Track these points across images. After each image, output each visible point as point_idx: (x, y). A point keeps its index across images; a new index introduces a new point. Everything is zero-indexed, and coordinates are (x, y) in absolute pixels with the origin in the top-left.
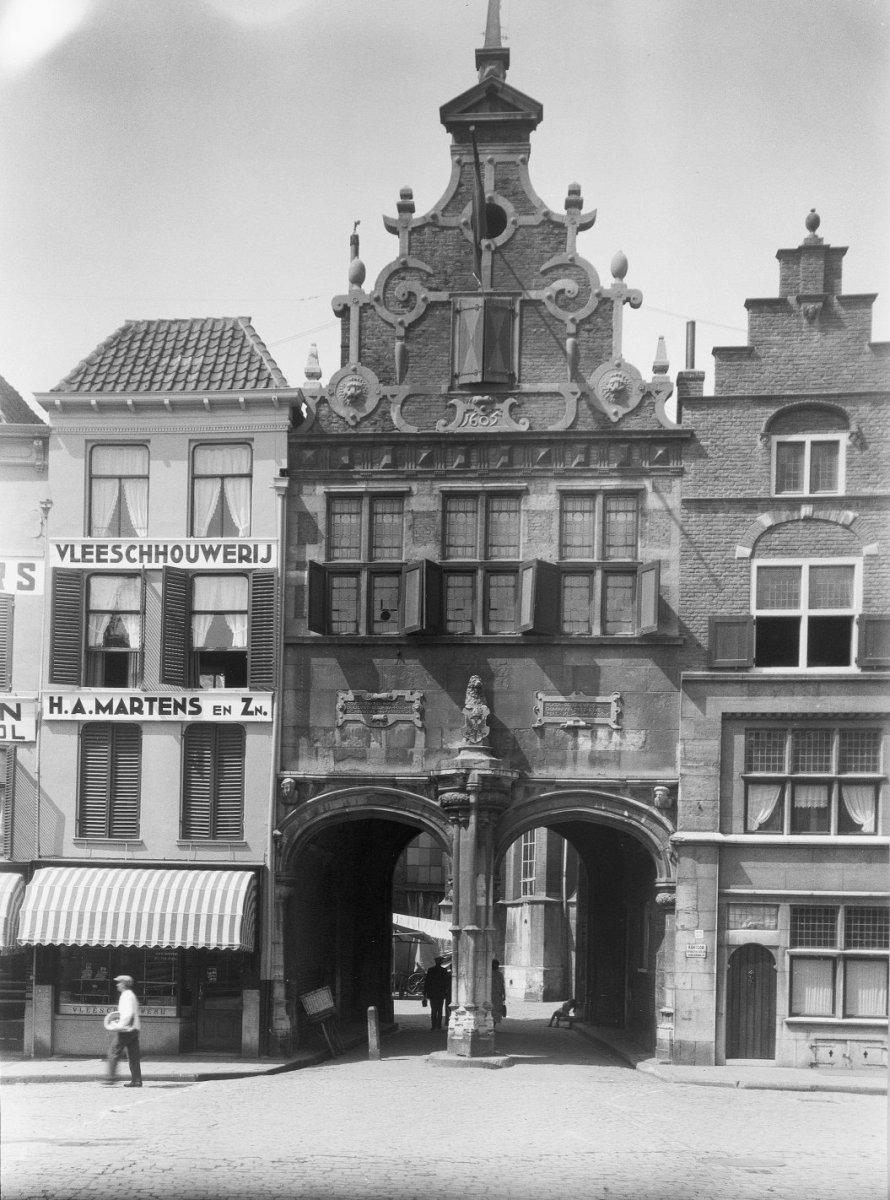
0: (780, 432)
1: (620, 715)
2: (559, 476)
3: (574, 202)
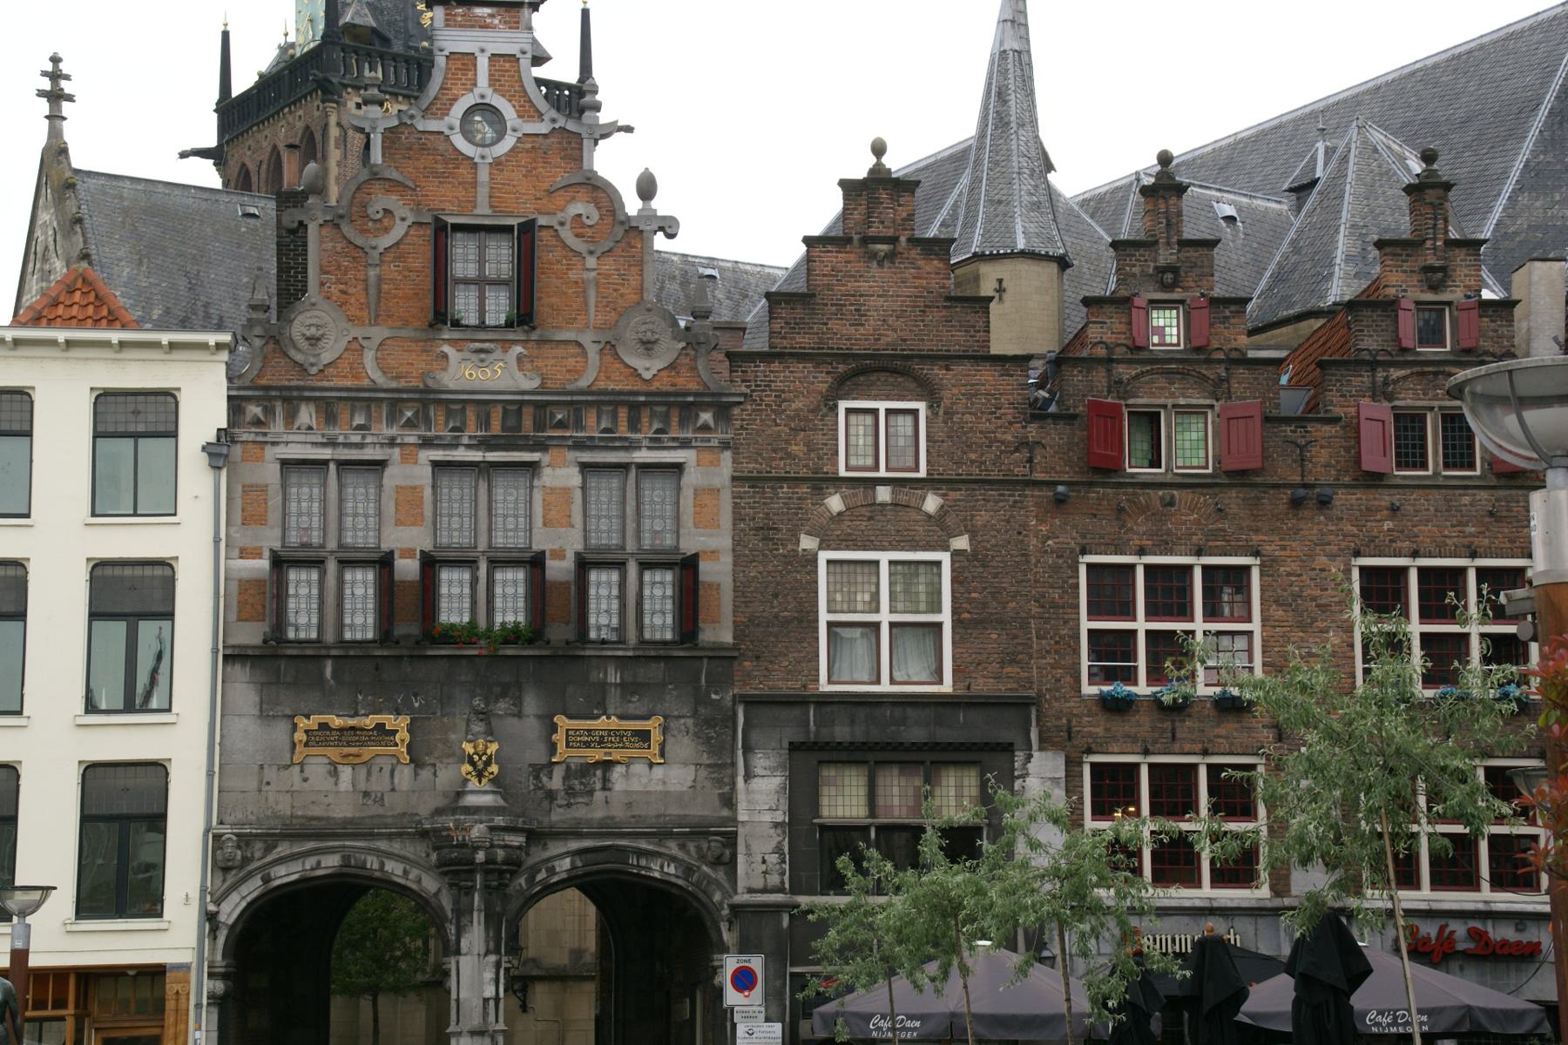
0: (846, 397)
1: (662, 746)
2: (579, 445)
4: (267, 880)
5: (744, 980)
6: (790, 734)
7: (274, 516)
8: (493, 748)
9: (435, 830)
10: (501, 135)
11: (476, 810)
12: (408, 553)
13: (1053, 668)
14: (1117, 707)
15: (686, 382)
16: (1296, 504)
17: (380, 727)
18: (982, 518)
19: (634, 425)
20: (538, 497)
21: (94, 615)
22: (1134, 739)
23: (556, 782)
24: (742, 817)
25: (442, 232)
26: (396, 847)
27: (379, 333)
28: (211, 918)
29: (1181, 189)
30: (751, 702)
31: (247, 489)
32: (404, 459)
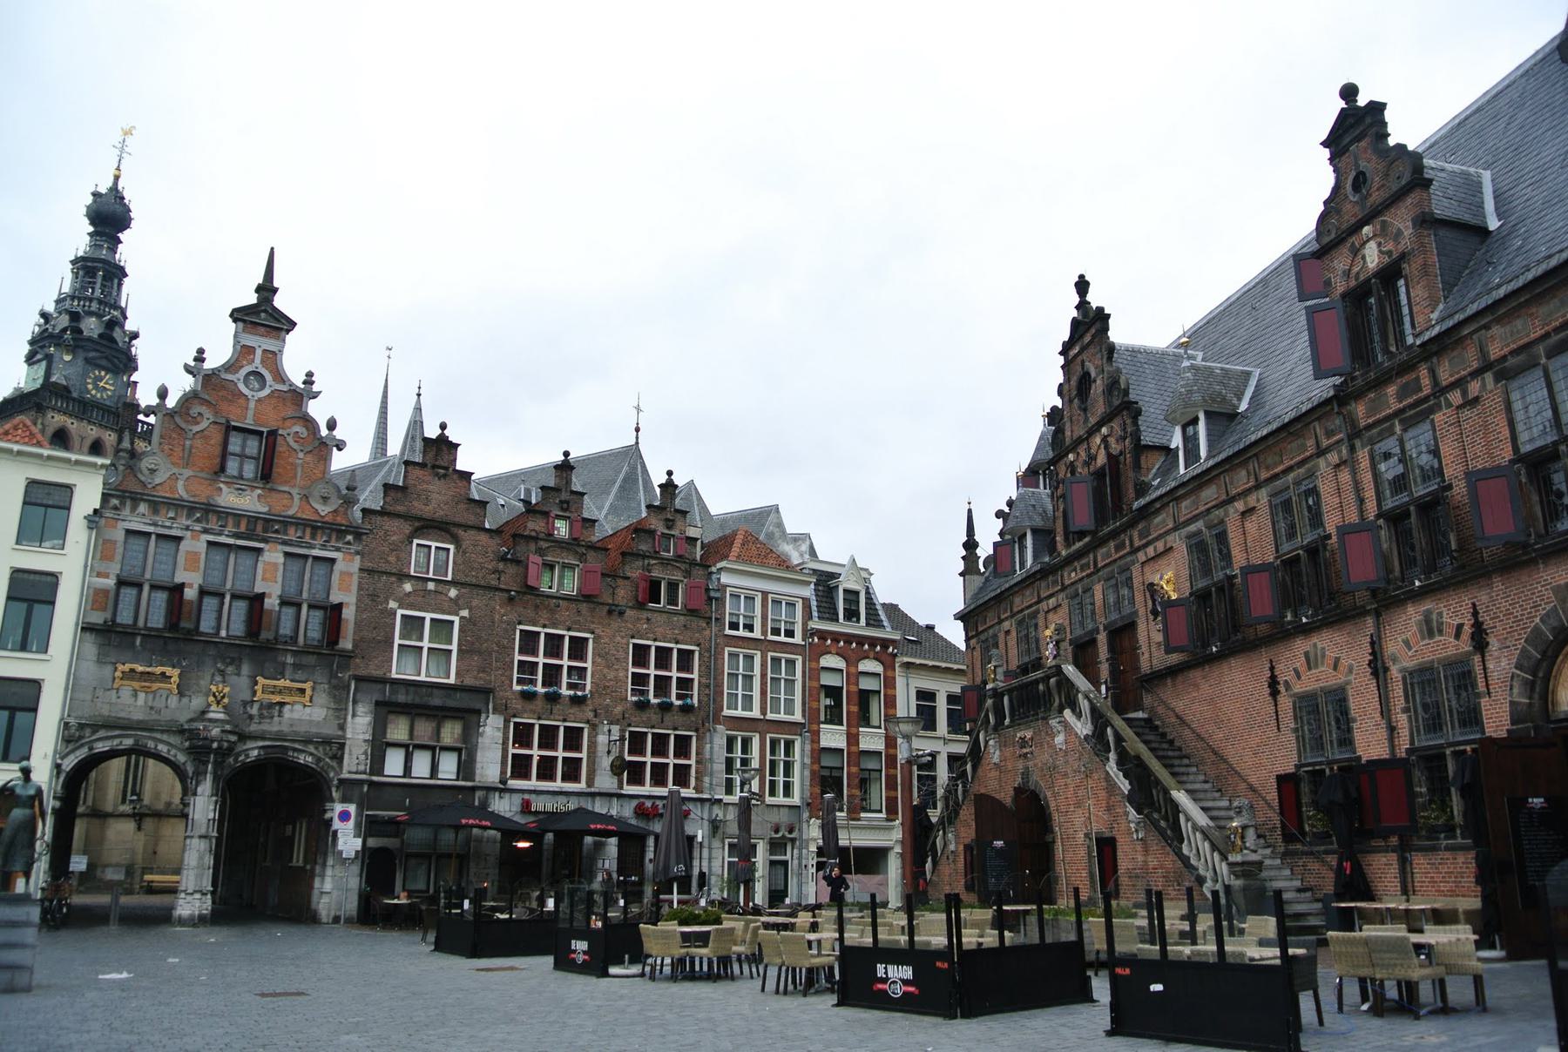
2: (285, 543)
3: (309, 381)
4: (91, 749)
5: (345, 816)
6: (376, 697)
7: (118, 557)
8: (227, 690)
9: (190, 730)
10: (263, 387)
11: (216, 721)
12: (191, 586)
14: (528, 696)
15: (339, 519)
16: (610, 612)
17: (163, 674)
18: (475, 603)
19: (313, 537)
20: (260, 565)
21: (9, 598)
23: (254, 711)
24: (349, 735)
25: (229, 429)
26: (165, 737)
27: (188, 473)
28: (58, 767)
29: (572, 468)
30: (359, 679)
31: (105, 542)
32: (193, 538)
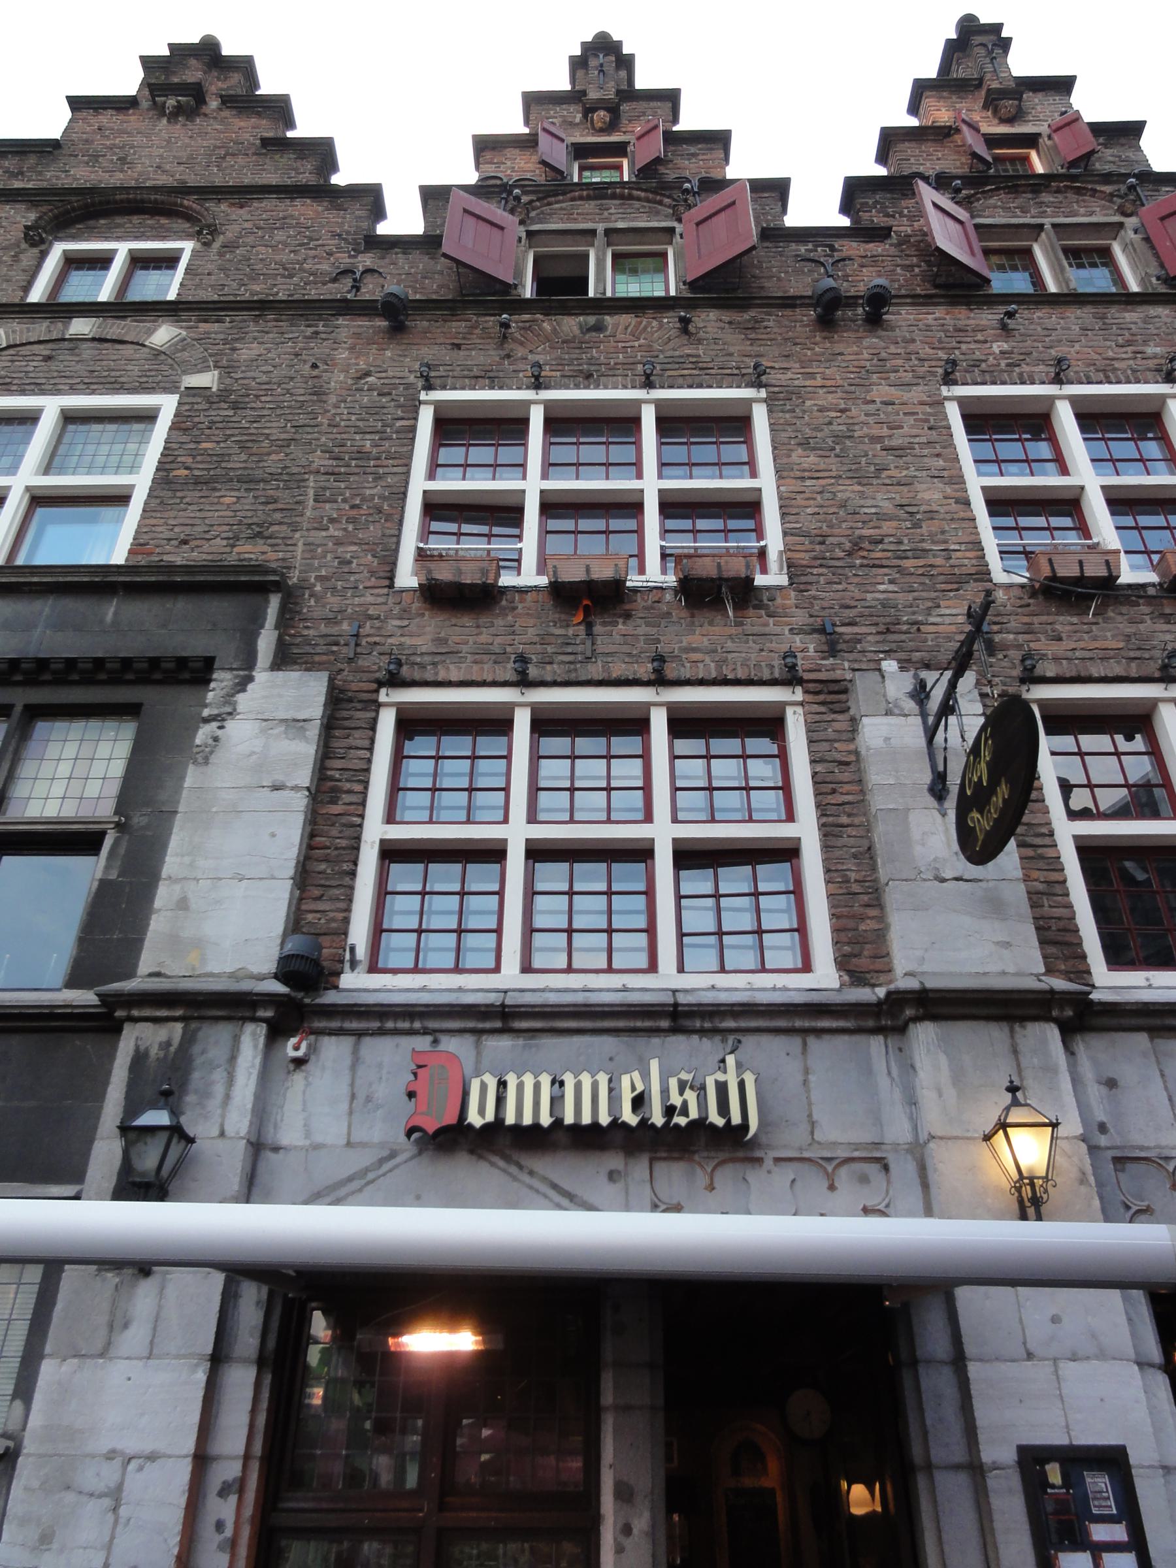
13: (338, 543)
22: (499, 657)
